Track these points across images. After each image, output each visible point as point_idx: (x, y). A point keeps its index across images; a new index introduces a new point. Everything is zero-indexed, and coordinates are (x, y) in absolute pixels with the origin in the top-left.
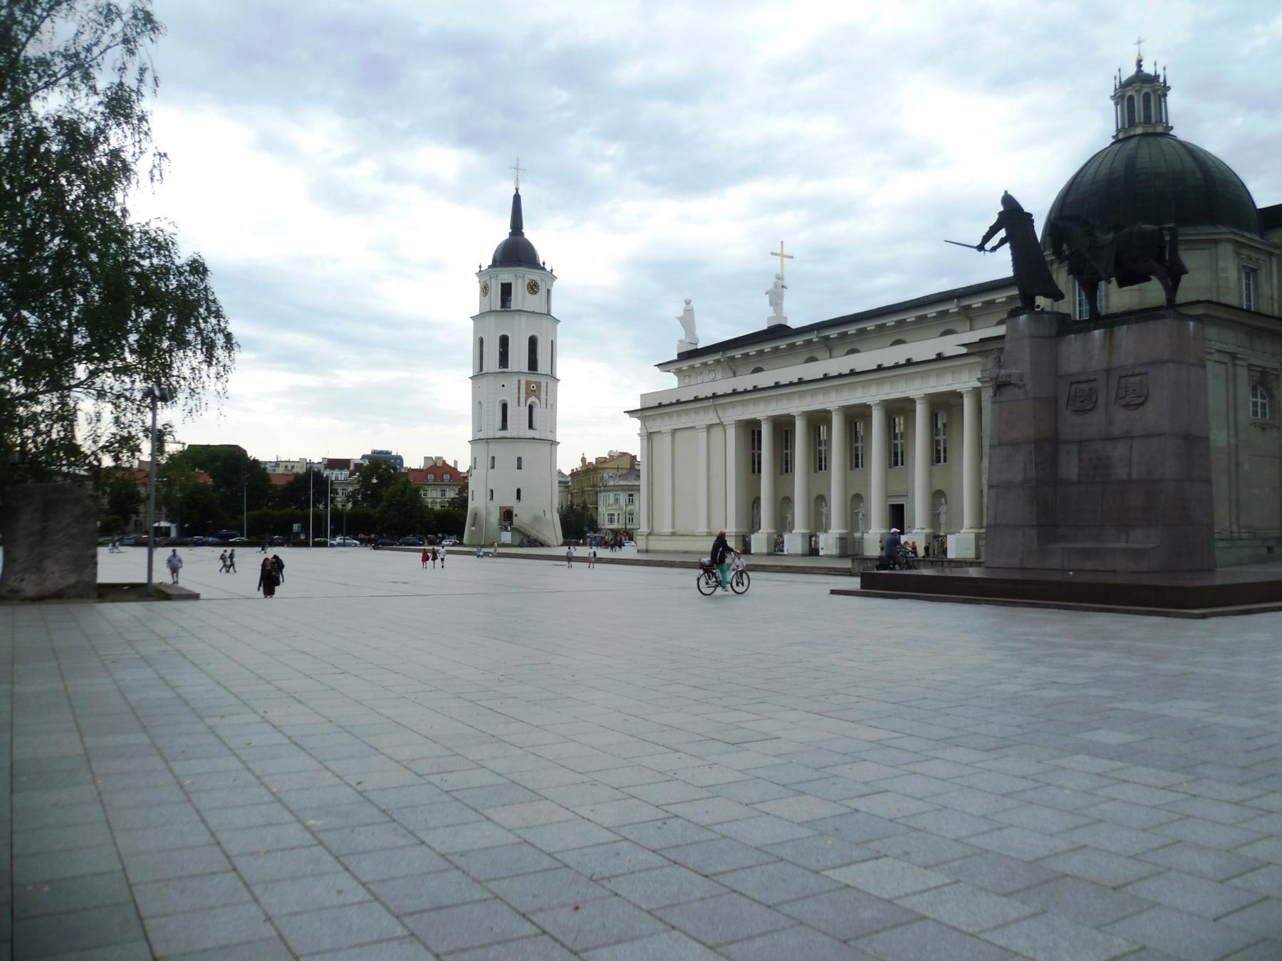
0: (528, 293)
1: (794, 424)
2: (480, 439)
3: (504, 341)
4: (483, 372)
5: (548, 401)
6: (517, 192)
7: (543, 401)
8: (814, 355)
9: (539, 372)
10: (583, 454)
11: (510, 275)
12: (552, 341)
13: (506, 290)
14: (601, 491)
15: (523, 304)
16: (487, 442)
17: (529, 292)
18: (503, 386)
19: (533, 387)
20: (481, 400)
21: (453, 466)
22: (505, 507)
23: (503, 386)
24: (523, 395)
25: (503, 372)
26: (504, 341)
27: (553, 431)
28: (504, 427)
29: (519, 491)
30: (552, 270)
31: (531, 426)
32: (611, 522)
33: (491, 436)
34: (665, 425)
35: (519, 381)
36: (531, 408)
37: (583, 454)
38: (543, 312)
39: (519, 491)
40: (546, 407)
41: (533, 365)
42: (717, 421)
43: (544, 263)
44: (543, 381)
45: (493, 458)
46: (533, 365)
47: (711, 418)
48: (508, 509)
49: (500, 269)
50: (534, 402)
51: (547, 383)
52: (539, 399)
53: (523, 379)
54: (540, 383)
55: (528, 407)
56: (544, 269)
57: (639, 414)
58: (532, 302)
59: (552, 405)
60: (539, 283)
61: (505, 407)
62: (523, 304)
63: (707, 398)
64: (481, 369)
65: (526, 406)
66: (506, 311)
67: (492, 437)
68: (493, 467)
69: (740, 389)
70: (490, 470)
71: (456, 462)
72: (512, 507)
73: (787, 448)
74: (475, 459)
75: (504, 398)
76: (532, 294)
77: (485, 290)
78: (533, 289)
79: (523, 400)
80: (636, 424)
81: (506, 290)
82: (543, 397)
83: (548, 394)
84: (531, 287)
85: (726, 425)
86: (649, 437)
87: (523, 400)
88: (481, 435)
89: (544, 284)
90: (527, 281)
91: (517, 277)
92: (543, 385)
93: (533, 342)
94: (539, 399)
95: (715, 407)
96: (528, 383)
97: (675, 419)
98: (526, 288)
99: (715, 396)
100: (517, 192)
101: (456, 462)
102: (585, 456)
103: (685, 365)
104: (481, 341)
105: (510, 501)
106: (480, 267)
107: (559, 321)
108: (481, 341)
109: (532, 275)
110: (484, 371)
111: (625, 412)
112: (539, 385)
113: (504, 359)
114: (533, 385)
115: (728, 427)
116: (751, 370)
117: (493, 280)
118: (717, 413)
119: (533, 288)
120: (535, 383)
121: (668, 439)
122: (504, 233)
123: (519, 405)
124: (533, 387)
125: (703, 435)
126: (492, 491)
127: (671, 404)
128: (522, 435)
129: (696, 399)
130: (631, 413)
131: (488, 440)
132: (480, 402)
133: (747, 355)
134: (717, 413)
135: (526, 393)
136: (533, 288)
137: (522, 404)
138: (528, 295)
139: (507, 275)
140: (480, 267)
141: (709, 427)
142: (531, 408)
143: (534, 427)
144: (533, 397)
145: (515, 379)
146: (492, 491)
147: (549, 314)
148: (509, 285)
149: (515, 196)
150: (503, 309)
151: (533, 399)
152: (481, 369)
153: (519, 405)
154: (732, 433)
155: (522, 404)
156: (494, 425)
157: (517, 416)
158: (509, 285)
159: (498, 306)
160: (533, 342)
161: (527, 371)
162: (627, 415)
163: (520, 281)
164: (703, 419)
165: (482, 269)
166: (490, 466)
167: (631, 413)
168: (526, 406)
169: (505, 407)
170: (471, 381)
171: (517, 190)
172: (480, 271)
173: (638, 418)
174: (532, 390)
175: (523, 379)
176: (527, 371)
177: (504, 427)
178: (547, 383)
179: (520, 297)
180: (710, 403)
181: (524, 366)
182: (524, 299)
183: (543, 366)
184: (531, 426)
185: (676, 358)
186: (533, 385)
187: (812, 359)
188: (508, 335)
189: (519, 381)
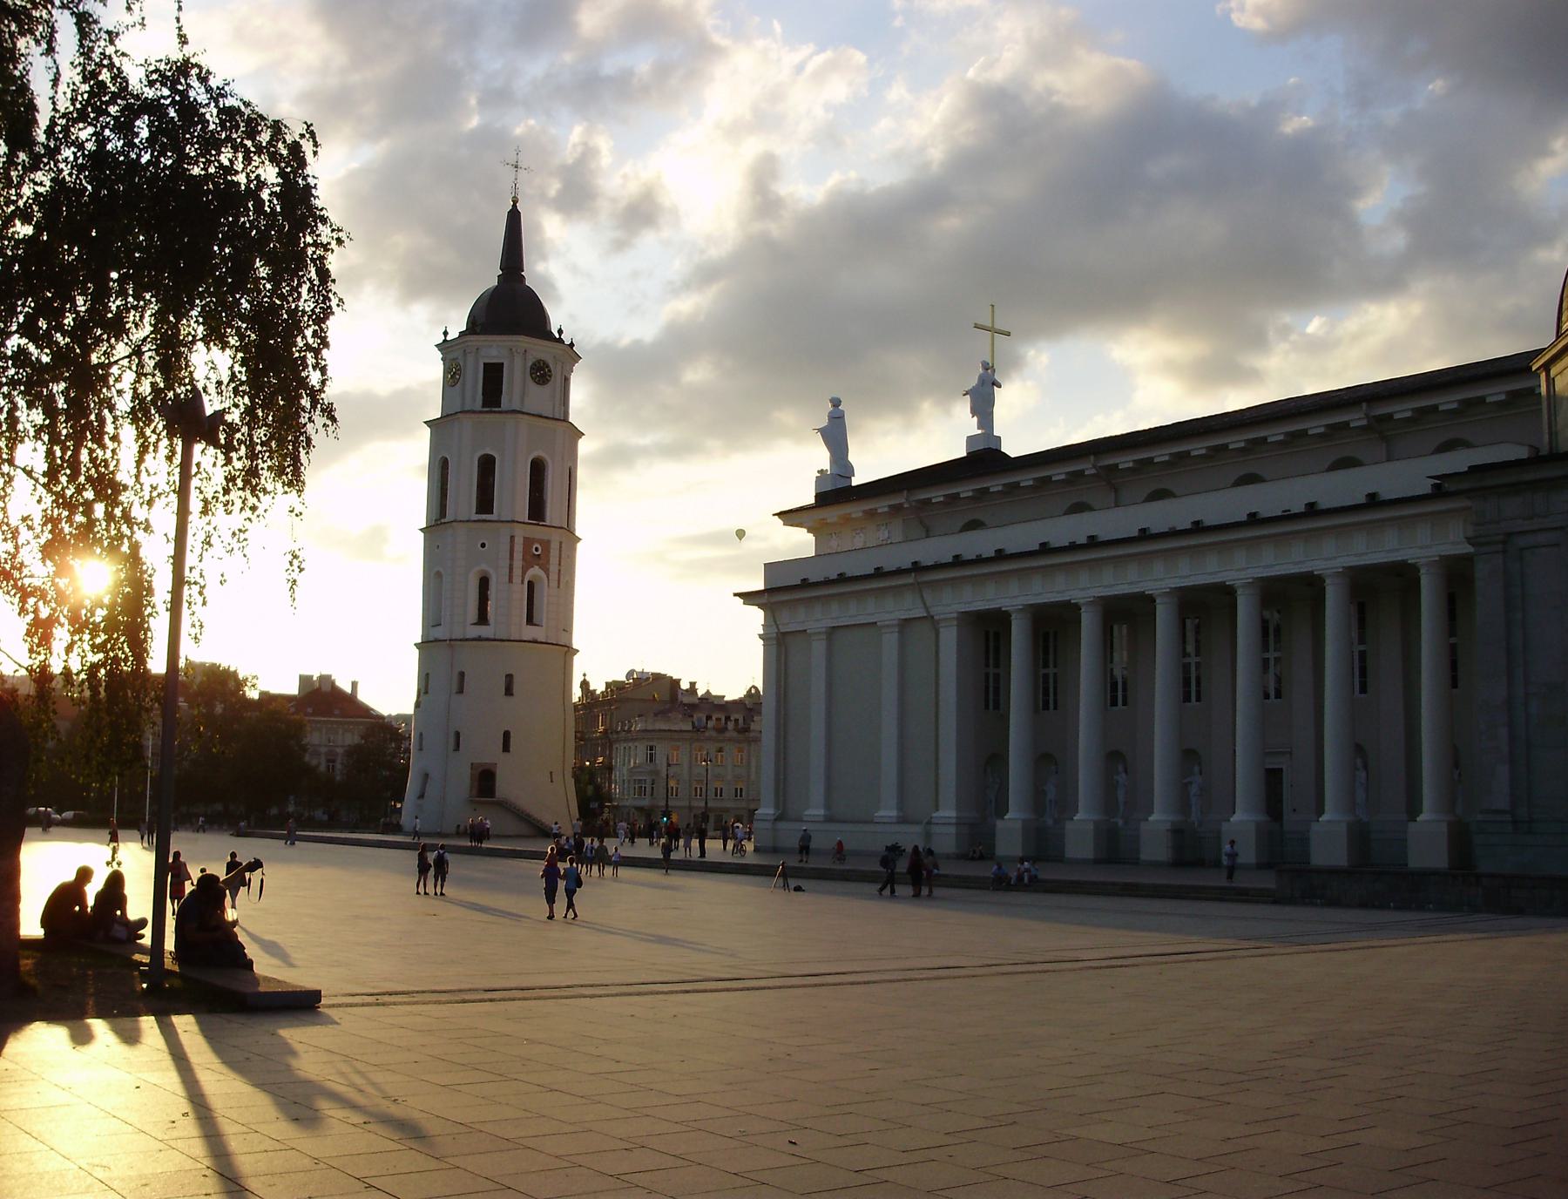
1: (1078, 622)
2: (436, 640)
3: (487, 466)
4: (446, 520)
5: (562, 579)
6: (514, 205)
7: (554, 576)
8: (978, 516)
10: (584, 675)
13: (493, 375)
14: (617, 741)
18: (483, 545)
19: (537, 549)
20: (441, 570)
21: (348, 689)
22: (480, 765)
23: (483, 545)
24: (518, 563)
26: (487, 466)
27: (568, 629)
28: (483, 618)
29: (507, 735)
30: (572, 345)
32: (640, 795)
33: (458, 634)
34: (816, 619)
35: (512, 537)
36: (531, 585)
37: (584, 675)
38: (557, 416)
39: (507, 735)
41: (537, 510)
42: (920, 613)
43: (560, 332)
44: (555, 537)
45: (462, 674)
47: (909, 606)
49: (482, 338)
51: (561, 543)
52: (547, 571)
53: (520, 533)
54: (549, 542)
55: (526, 582)
56: (560, 341)
57: (764, 599)
58: (538, 397)
61: (484, 583)
63: (899, 572)
64: (443, 513)
65: (522, 582)
66: (491, 412)
68: (461, 691)
69: (969, 555)
71: (354, 685)
73: (1046, 665)
74: (427, 674)
75: (484, 567)
77: (453, 375)
79: (517, 572)
80: (756, 616)
81: (493, 375)
82: (553, 568)
85: (938, 622)
86: (778, 644)
87: (517, 572)
88: (439, 633)
90: (530, 364)
92: (554, 546)
93: (538, 468)
94: (547, 571)
95: (919, 588)
96: (528, 542)
97: (835, 607)
99: (917, 568)
100: (514, 205)
101: (354, 685)
102: (587, 678)
103: (832, 514)
105: (490, 753)
106: (446, 333)
107: (583, 434)
108: (444, 464)
109: (538, 349)
111: (735, 595)
112: (546, 544)
113: (485, 502)
115: (941, 625)
116: (960, 524)
117: (470, 359)
118: (922, 597)
120: (541, 542)
121: (818, 648)
122: (489, 277)
123: (510, 581)
124: (537, 549)
125: (890, 640)
126: (458, 734)
127: (828, 583)
129: (879, 573)
130: (748, 597)
132: (439, 574)
133: (955, 497)
134: (922, 597)
135: (524, 559)
136: (541, 373)
138: (533, 388)
139: (495, 348)
140: (446, 333)
141: (905, 623)
142: (531, 585)
143: (535, 621)
144: (537, 567)
145: (505, 531)
147: (566, 420)
150: (485, 409)
151: (535, 571)
152: (443, 513)
153: (510, 581)
154: (949, 638)
157: (507, 601)
160: (538, 468)
161: (527, 521)
162: (740, 601)
163: (518, 361)
164: (891, 610)
165: (449, 338)
166: (455, 687)
167: (748, 597)
168: (522, 582)
169: (484, 583)
170: (422, 534)
171: (515, 202)
172: (445, 341)
173: (760, 606)
174: (534, 555)
175: (520, 533)
177: (483, 618)
178: (561, 543)
179: (515, 385)
180: (910, 579)
181: (523, 512)
183: (552, 512)
184: (530, 620)
185: (812, 501)
187: (1079, 508)
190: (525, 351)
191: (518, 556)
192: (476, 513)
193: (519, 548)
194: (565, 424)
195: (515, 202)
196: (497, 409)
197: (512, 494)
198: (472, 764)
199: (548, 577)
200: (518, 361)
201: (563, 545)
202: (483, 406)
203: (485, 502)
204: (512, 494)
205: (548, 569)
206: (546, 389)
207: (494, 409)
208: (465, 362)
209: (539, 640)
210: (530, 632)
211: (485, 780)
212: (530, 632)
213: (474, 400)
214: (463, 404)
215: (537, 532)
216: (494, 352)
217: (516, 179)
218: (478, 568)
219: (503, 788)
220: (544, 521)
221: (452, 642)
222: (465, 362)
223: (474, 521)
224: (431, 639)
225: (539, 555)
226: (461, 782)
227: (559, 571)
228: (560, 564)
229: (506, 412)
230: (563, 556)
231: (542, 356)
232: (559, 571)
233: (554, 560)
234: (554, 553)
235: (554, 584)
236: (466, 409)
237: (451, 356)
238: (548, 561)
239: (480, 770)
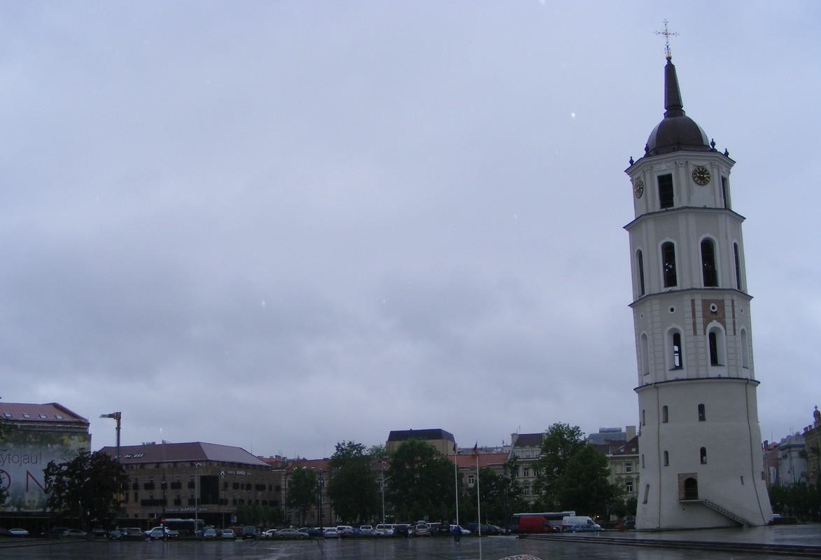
2: (647, 385)
3: (668, 252)
4: (645, 295)
5: (737, 328)
7: (729, 326)
9: (720, 287)
12: (735, 246)
13: (665, 184)
15: (689, 200)
16: (657, 388)
17: (696, 182)
18: (672, 310)
19: (713, 308)
22: (685, 475)
23: (672, 310)
24: (700, 320)
25: (671, 292)
26: (668, 250)
27: (748, 364)
29: (703, 452)
31: (714, 361)
35: (693, 301)
36: (713, 337)
38: (719, 206)
39: (703, 452)
40: (735, 334)
41: (710, 277)
43: (713, 144)
45: (666, 408)
46: (710, 277)
48: (688, 477)
50: (715, 328)
51: (733, 301)
52: (724, 324)
54: (723, 300)
56: (714, 150)
59: (743, 331)
62: (689, 200)
66: (667, 210)
67: (663, 380)
68: (666, 421)
70: (663, 425)
72: (696, 474)
74: (644, 411)
75: (674, 326)
78: (703, 179)
79: (700, 326)
81: (665, 184)
82: (729, 320)
83: (736, 315)
84: (700, 178)
87: (700, 326)
88: (649, 380)
89: (715, 171)
90: (691, 169)
91: (679, 167)
92: (728, 303)
93: (708, 249)
94: (724, 324)
96: (706, 303)
98: (691, 179)
104: (640, 254)
105: (691, 466)
108: (640, 254)
109: (698, 160)
110: (647, 293)
112: (721, 304)
113: (670, 279)
114: (712, 305)
117: (648, 176)
119: (701, 177)
120: (716, 301)
122: (658, 114)
123: (695, 333)
124: (713, 308)
126: (666, 453)
128: (703, 374)
131: (656, 385)
137: (700, 332)
138: (696, 188)
142: (713, 337)
144: (715, 321)
145: (687, 300)
146: (666, 453)
147: (727, 207)
148: (669, 176)
150: (664, 209)
151: (714, 324)
153: (695, 333)
155: (700, 332)
156: (664, 363)
157: (694, 346)
158: (669, 176)
159: (657, 207)
160: (708, 249)
163: (682, 171)
166: (662, 419)
168: (705, 334)
176: (703, 286)
178: (733, 301)
181: (699, 281)
182: (690, 192)
183: (725, 277)
184: (714, 361)
186: (712, 305)
189: (693, 301)
190: (687, 162)
191: (699, 314)
192: (665, 287)
193: (699, 308)
194: (727, 212)
195: (669, 59)
196: (672, 208)
197: (690, 270)
198: (679, 475)
199: (725, 328)
201: (735, 302)
202: (663, 206)
203: (670, 279)
204: (690, 270)
205: (725, 322)
207: (669, 209)
208: (645, 178)
209: (722, 376)
210: (714, 372)
211: (690, 486)
213: (654, 205)
214: (647, 208)
215: (711, 296)
217: (668, 42)
218: (670, 328)
219: (702, 494)
220: (717, 286)
221: (657, 385)
222: (645, 178)
223: (664, 293)
224: (644, 384)
225: (716, 312)
226: (672, 493)
227: (734, 322)
228: (734, 317)
229: (678, 209)
230: (736, 310)
231: (700, 163)
232: (734, 322)
233: (728, 314)
234: (728, 309)
235: (730, 332)
236: (650, 212)
237: (635, 177)
238: (724, 317)
239: (686, 478)
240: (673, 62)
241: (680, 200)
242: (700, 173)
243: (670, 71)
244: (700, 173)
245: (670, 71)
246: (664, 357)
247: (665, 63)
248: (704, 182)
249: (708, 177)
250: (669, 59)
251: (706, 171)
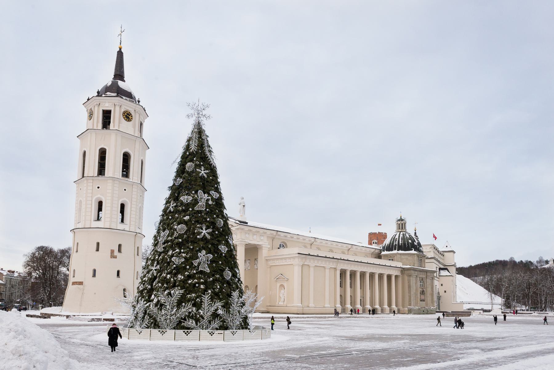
0: (123, 119)
3: (103, 154)
11: (110, 104)
13: (107, 116)
17: (124, 118)
18: (98, 188)
26: (103, 154)
60: (133, 114)
76: (126, 120)
78: (128, 118)
81: (107, 116)
84: (126, 116)
89: (137, 115)
90: (123, 110)
117: (96, 108)
119: (128, 116)
138: (123, 121)
139: (108, 103)
149: (118, 52)
163: (117, 108)
188: (105, 147)
195: (120, 49)
200: (117, 108)
206: (130, 123)
212: (121, 226)
213: (97, 126)
216: (107, 105)
240: (122, 50)
241: (114, 126)
242: (127, 114)
243: (120, 54)
244: (127, 114)
245: (120, 54)
246: (91, 216)
247: (118, 49)
248: (129, 120)
249: (132, 118)
250: (120, 49)
251: (131, 114)
